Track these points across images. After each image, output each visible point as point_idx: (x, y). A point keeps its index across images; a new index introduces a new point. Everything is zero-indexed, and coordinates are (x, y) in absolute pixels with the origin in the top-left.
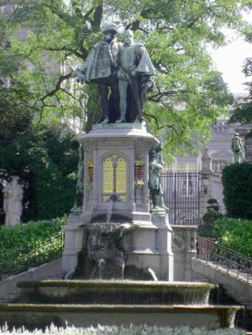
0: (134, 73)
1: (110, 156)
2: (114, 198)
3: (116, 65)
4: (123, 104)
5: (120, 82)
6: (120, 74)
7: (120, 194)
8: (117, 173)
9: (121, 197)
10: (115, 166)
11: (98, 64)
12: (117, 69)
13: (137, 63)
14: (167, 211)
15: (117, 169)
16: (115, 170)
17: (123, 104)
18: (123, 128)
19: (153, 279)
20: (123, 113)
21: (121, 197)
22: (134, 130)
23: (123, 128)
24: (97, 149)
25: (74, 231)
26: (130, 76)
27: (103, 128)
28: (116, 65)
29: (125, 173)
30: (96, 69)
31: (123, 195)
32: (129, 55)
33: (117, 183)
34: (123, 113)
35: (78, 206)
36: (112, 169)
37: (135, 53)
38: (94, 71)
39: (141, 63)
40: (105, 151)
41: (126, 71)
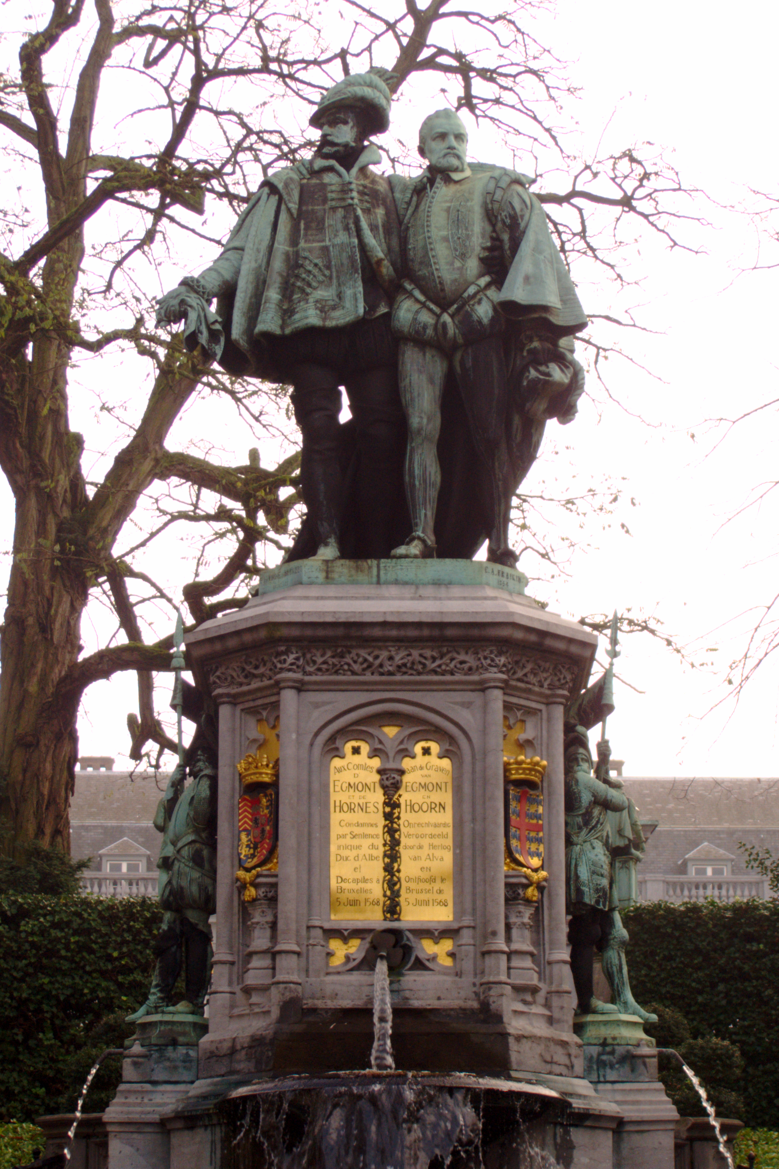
0: (483, 311)
3: (387, 270)
8: (405, 816)
9: (428, 948)
11: (294, 263)
14: (648, 1028)
15: (405, 797)
16: (392, 806)
21: (428, 948)
24: (300, 688)
27: (328, 578)
28: (387, 270)
29: (447, 817)
30: (287, 290)
32: (458, 219)
33: (408, 867)
35: (170, 998)
36: (378, 797)
37: (490, 215)
38: (273, 294)
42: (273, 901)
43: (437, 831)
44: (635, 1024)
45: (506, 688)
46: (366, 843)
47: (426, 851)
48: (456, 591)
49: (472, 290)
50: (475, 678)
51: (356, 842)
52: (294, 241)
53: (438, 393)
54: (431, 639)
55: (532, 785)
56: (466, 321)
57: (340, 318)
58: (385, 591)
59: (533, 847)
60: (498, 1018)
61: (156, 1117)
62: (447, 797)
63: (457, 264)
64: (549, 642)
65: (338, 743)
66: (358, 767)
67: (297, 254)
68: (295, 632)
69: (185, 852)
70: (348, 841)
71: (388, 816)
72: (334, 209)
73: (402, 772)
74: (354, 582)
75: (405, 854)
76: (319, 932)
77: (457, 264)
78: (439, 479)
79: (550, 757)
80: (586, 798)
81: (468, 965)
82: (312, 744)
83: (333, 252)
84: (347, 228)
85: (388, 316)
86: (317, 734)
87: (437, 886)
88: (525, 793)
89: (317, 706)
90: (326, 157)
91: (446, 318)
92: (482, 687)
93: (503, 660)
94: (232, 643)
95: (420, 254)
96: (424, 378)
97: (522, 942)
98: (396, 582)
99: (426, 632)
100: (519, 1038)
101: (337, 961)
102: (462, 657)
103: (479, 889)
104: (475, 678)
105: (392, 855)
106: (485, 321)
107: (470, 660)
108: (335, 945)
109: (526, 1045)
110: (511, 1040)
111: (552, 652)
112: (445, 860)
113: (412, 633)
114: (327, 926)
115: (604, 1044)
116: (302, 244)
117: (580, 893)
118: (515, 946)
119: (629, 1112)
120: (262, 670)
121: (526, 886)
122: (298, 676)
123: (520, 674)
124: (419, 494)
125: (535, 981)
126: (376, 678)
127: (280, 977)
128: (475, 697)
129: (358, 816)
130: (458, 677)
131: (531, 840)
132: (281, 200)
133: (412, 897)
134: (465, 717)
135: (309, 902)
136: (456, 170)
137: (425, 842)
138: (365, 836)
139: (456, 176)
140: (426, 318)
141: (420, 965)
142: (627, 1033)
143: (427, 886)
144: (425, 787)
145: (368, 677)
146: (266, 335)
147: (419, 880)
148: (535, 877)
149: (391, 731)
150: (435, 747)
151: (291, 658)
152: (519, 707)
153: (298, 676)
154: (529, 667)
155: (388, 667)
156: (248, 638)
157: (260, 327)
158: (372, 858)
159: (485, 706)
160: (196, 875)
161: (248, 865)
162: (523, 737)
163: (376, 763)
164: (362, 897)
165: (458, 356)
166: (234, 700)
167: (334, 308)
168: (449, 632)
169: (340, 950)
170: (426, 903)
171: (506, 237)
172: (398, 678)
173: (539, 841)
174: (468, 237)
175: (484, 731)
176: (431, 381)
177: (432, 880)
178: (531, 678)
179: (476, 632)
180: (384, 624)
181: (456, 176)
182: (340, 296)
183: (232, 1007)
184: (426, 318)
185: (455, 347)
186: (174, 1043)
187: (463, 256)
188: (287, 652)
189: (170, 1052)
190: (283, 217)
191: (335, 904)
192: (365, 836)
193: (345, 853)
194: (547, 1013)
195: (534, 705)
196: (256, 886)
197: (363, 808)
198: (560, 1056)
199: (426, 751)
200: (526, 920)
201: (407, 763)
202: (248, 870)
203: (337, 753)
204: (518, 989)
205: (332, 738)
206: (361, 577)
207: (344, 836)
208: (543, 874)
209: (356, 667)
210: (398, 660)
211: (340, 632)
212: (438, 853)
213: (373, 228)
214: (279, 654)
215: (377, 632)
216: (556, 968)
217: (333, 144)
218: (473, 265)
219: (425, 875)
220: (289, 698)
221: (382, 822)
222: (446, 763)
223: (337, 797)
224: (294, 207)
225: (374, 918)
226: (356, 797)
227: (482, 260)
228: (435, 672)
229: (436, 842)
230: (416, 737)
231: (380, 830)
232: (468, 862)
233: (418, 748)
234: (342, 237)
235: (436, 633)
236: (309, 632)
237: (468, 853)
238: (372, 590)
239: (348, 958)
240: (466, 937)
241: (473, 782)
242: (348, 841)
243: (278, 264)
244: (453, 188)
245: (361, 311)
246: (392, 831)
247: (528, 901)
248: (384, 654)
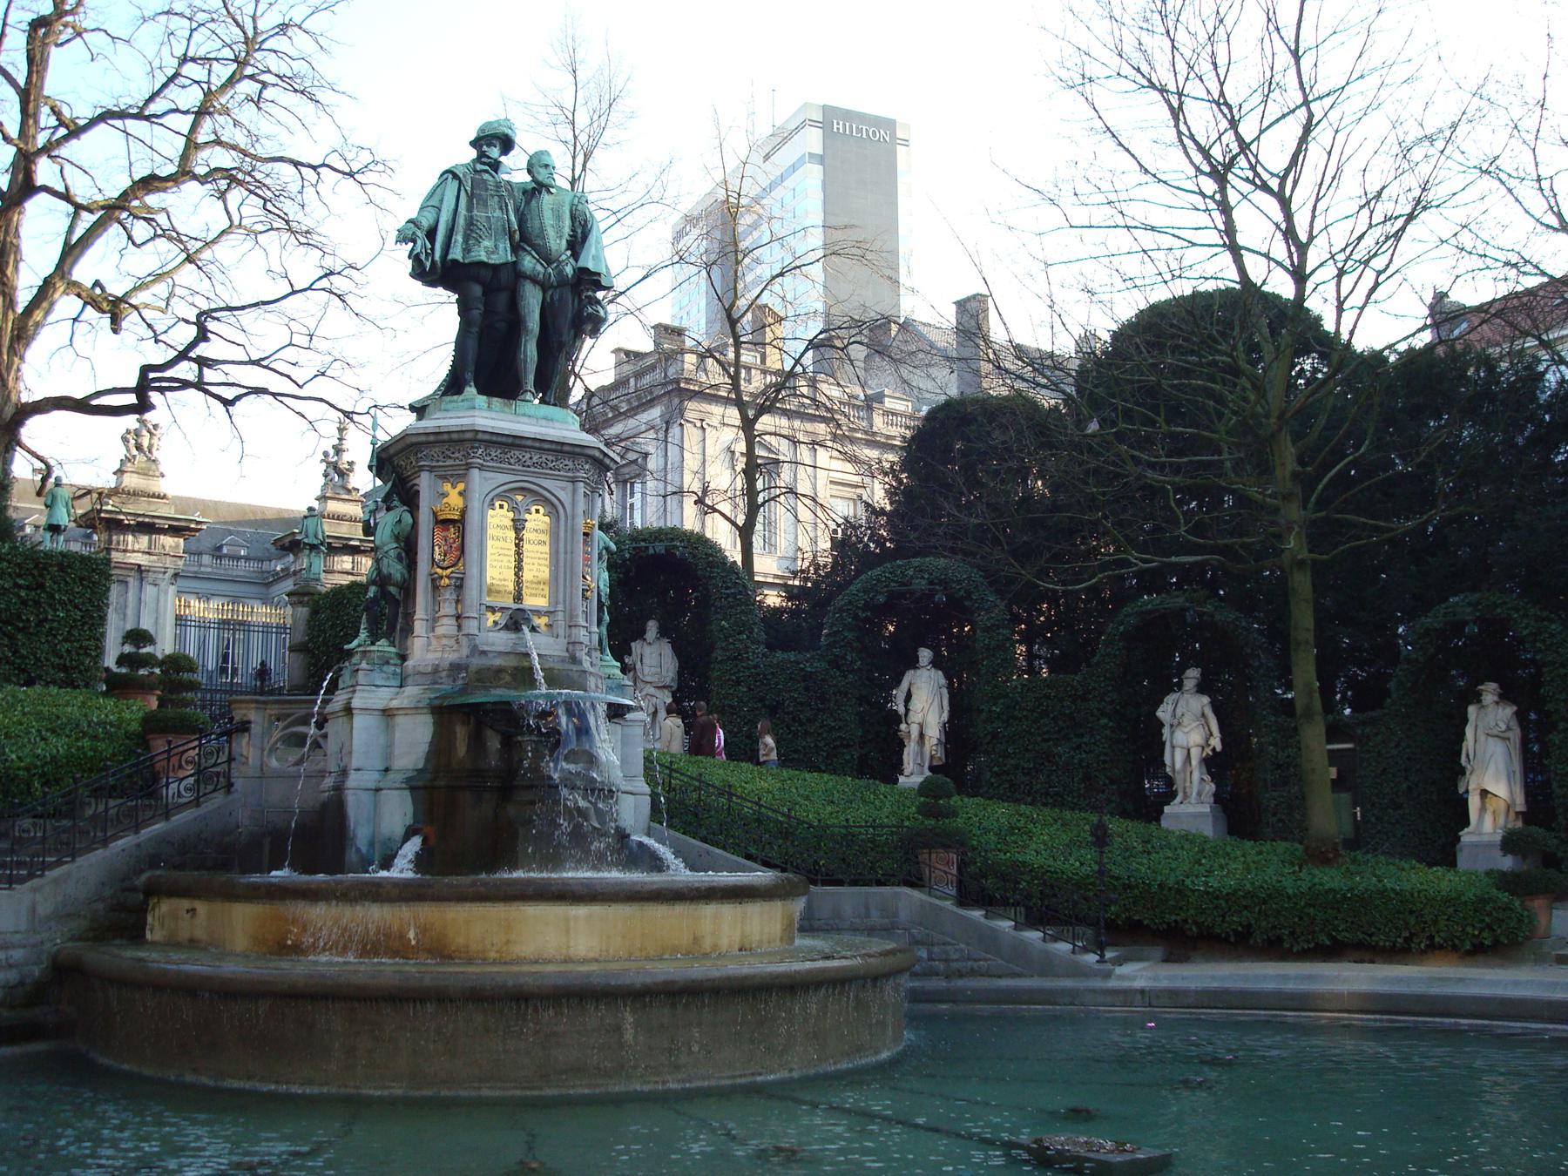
0: (569, 270)
1: (505, 496)
2: (517, 620)
4: (530, 351)
6: (529, 263)
8: (526, 547)
10: (518, 526)
11: (470, 222)
15: (526, 535)
17: (530, 351)
23: (545, 418)
24: (481, 468)
25: (387, 714)
29: (546, 549)
30: (466, 238)
33: (527, 575)
38: (459, 238)
42: (460, 586)
47: (536, 566)
48: (557, 425)
50: (570, 474)
51: (500, 558)
52: (470, 208)
56: (560, 273)
57: (495, 259)
61: (381, 707)
62: (546, 538)
67: (472, 217)
68: (487, 437)
69: (392, 553)
70: (496, 557)
71: (517, 545)
72: (492, 196)
76: (483, 607)
78: (536, 358)
84: (501, 208)
87: (542, 586)
90: (484, 164)
92: (574, 481)
94: (446, 437)
95: (537, 231)
98: (524, 415)
99: (553, 447)
101: (490, 623)
103: (568, 591)
104: (570, 474)
105: (519, 568)
107: (570, 463)
108: (489, 614)
112: (545, 573)
113: (546, 446)
116: (475, 212)
120: (457, 455)
128: (570, 485)
129: (501, 544)
132: (460, 182)
133: (529, 591)
134: (562, 495)
137: (536, 561)
145: (517, 467)
146: (455, 261)
147: (532, 582)
150: (542, 510)
156: (455, 436)
157: (450, 257)
159: (574, 491)
160: (399, 567)
161: (446, 564)
163: (511, 515)
164: (502, 589)
165: (550, 292)
166: (431, 469)
167: (493, 253)
168: (566, 448)
169: (491, 618)
171: (579, 231)
172: (532, 469)
175: (573, 505)
177: (539, 583)
180: (534, 439)
183: (429, 644)
184: (539, 268)
185: (552, 286)
186: (387, 663)
187: (561, 237)
189: (385, 668)
190: (463, 194)
191: (490, 592)
193: (495, 564)
196: (448, 577)
197: (505, 540)
199: (537, 511)
201: (527, 516)
202: (442, 568)
203: (492, 506)
206: (506, 409)
209: (512, 461)
210: (534, 460)
211: (510, 440)
214: (473, 448)
215: (529, 443)
217: (489, 157)
218: (564, 243)
219: (535, 580)
221: (514, 548)
223: (490, 532)
224: (469, 189)
225: (509, 602)
226: (500, 533)
230: (535, 502)
232: (561, 575)
233: (533, 509)
234: (498, 213)
235: (559, 448)
236: (494, 438)
237: (562, 570)
238: (511, 417)
239: (496, 623)
240: (560, 616)
241: (566, 531)
242: (496, 557)
243: (461, 221)
244: (551, 197)
248: (528, 456)
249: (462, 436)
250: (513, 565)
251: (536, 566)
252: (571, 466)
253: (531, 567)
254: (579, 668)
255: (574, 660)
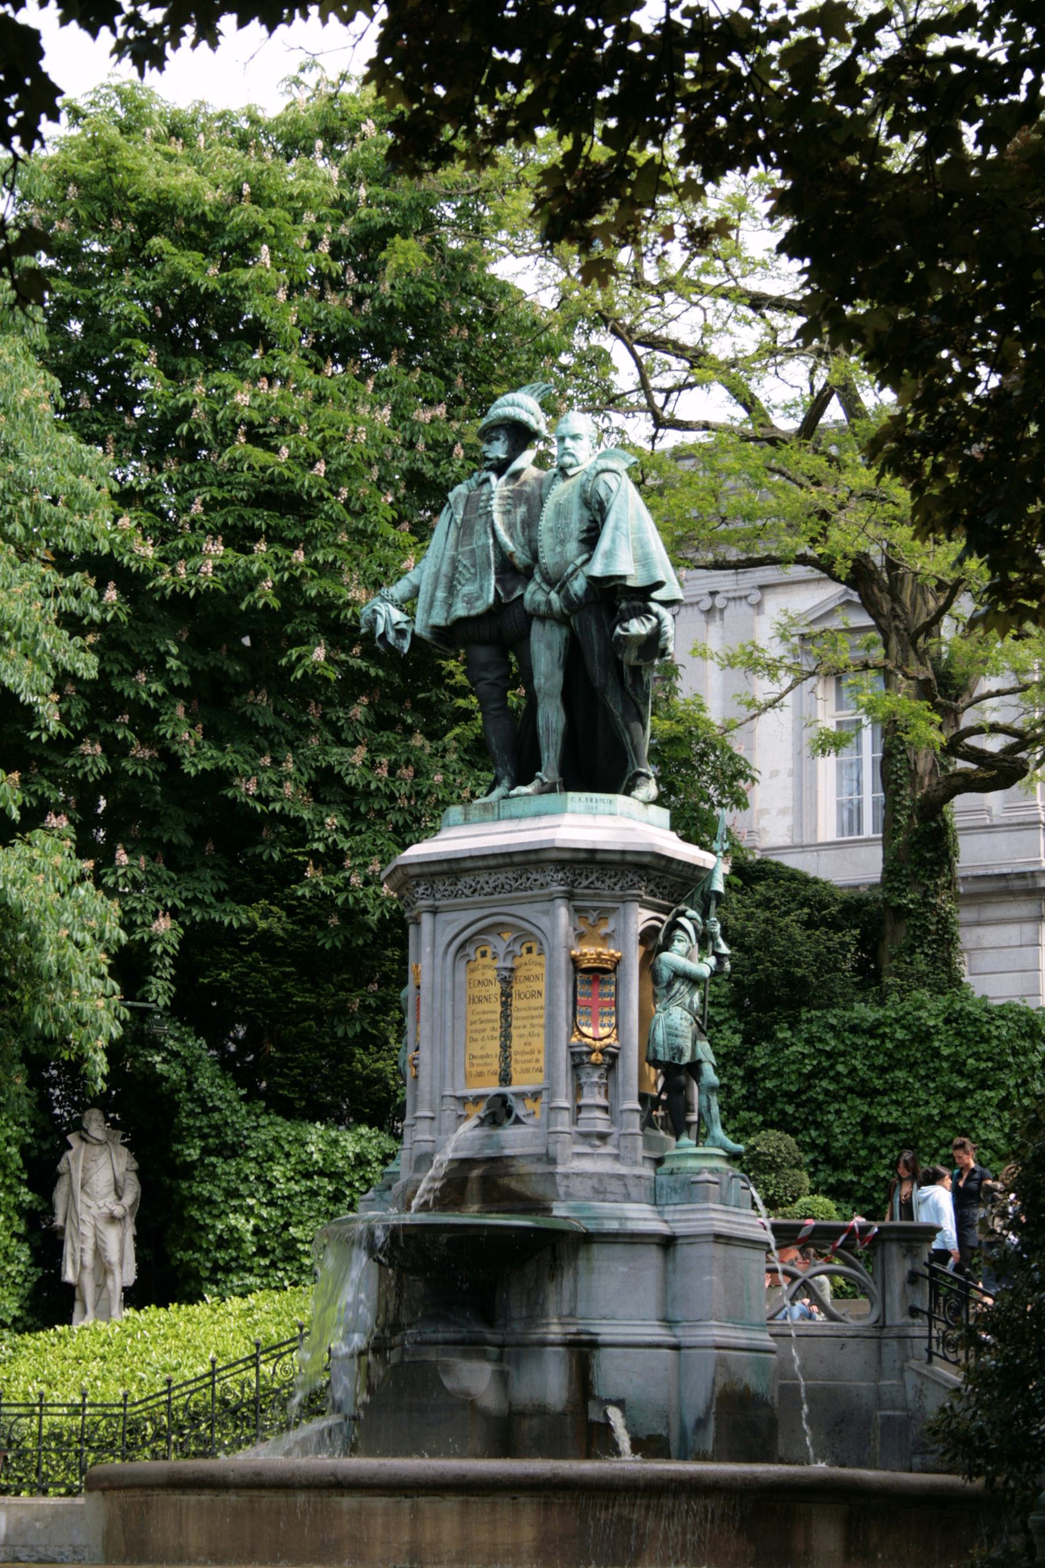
0: (578, 586)
5: (536, 628)
7: (521, 1096)
8: (516, 1003)
12: (527, 575)
13: (591, 539)
15: (518, 988)
18: (538, 815)
19: (613, 1449)
20: (550, 757)
22: (567, 819)
24: (434, 911)
26: (567, 599)
28: (521, 558)
29: (541, 1001)
31: (536, 1095)
33: (516, 1044)
34: (550, 757)
36: (496, 989)
37: (586, 503)
38: (441, 594)
39: (604, 543)
40: (466, 917)
41: (557, 581)
43: (535, 1013)
44: (718, 1156)
45: (570, 897)
46: (488, 1026)
49: (570, 569)
53: (556, 655)
54: (498, 867)
55: (606, 971)
57: (479, 607)
58: (504, 826)
59: (606, 1020)
60: (552, 1160)
63: (558, 549)
64: (599, 856)
65: (470, 949)
66: (484, 967)
68: (416, 871)
73: (512, 970)
74: (483, 821)
75: (514, 1032)
77: (558, 549)
79: (625, 945)
80: (666, 974)
81: (544, 1119)
82: (446, 952)
83: (478, 552)
85: (522, 596)
86: (449, 944)
87: (536, 1056)
88: (596, 979)
89: (449, 923)
91: (553, 596)
93: (560, 875)
96: (542, 646)
97: (594, 1097)
98: (511, 818)
99: (501, 861)
100: (566, 1176)
102: (534, 876)
105: (506, 1036)
106: (580, 593)
107: (541, 880)
109: (576, 1182)
110: (558, 1178)
111: (612, 863)
113: (492, 862)
114: (459, 1093)
115: (672, 1173)
117: (655, 1052)
118: (583, 1101)
119: (680, 1229)
121: (589, 1053)
122: (430, 902)
123: (585, 883)
124: (543, 742)
125: (602, 1127)
126: (482, 898)
127: (419, 1137)
129: (484, 1006)
130: (536, 892)
131: (604, 1014)
134: (544, 922)
135: (443, 1077)
136: (571, 466)
137: (527, 1022)
138: (489, 1021)
139: (570, 472)
140: (540, 597)
141: (518, 1121)
142: (691, 1163)
143: (528, 1057)
144: (528, 978)
145: (476, 898)
147: (524, 1053)
148: (598, 1044)
149: (508, 937)
151: (421, 890)
152: (595, 909)
153: (430, 902)
154: (592, 878)
155: (487, 890)
158: (493, 1038)
162: (604, 930)
164: (485, 1069)
167: (478, 598)
168: (517, 859)
170: (528, 1071)
172: (496, 896)
173: (610, 1014)
174: (567, 525)
176: (549, 647)
177: (532, 1052)
178: (598, 884)
179: (533, 857)
180: (471, 858)
181: (570, 472)
182: (481, 587)
187: (563, 542)
188: (418, 885)
192: (489, 1021)
194: (615, 1151)
195: (609, 905)
197: (487, 999)
198: (615, 1186)
199: (529, 950)
200: (595, 1079)
201: (518, 961)
204: (586, 1136)
205: (462, 946)
206: (488, 816)
207: (473, 1023)
208: (607, 1041)
209: (467, 892)
211: (445, 867)
212: (536, 1030)
213: (510, 527)
215: (469, 864)
216: (625, 1115)
218: (572, 547)
219: (528, 1049)
220: (426, 919)
221: (498, 1008)
222: (542, 959)
224: (459, 517)
227: (582, 541)
228: (517, 889)
229: (536, 1021)
231: (497, 1016)
235: (508, 860)
236: (426, 869)
245: (491, 599)
246: (506, 1016)
247: (596, 1066)
248: (482, 880)
249: (455, 866)
250: (497, 1034)
251: (526, 1031)
252: (541, 880)
253: (522, 1031)
254: (550, 1169)
255: (550, 1160)
